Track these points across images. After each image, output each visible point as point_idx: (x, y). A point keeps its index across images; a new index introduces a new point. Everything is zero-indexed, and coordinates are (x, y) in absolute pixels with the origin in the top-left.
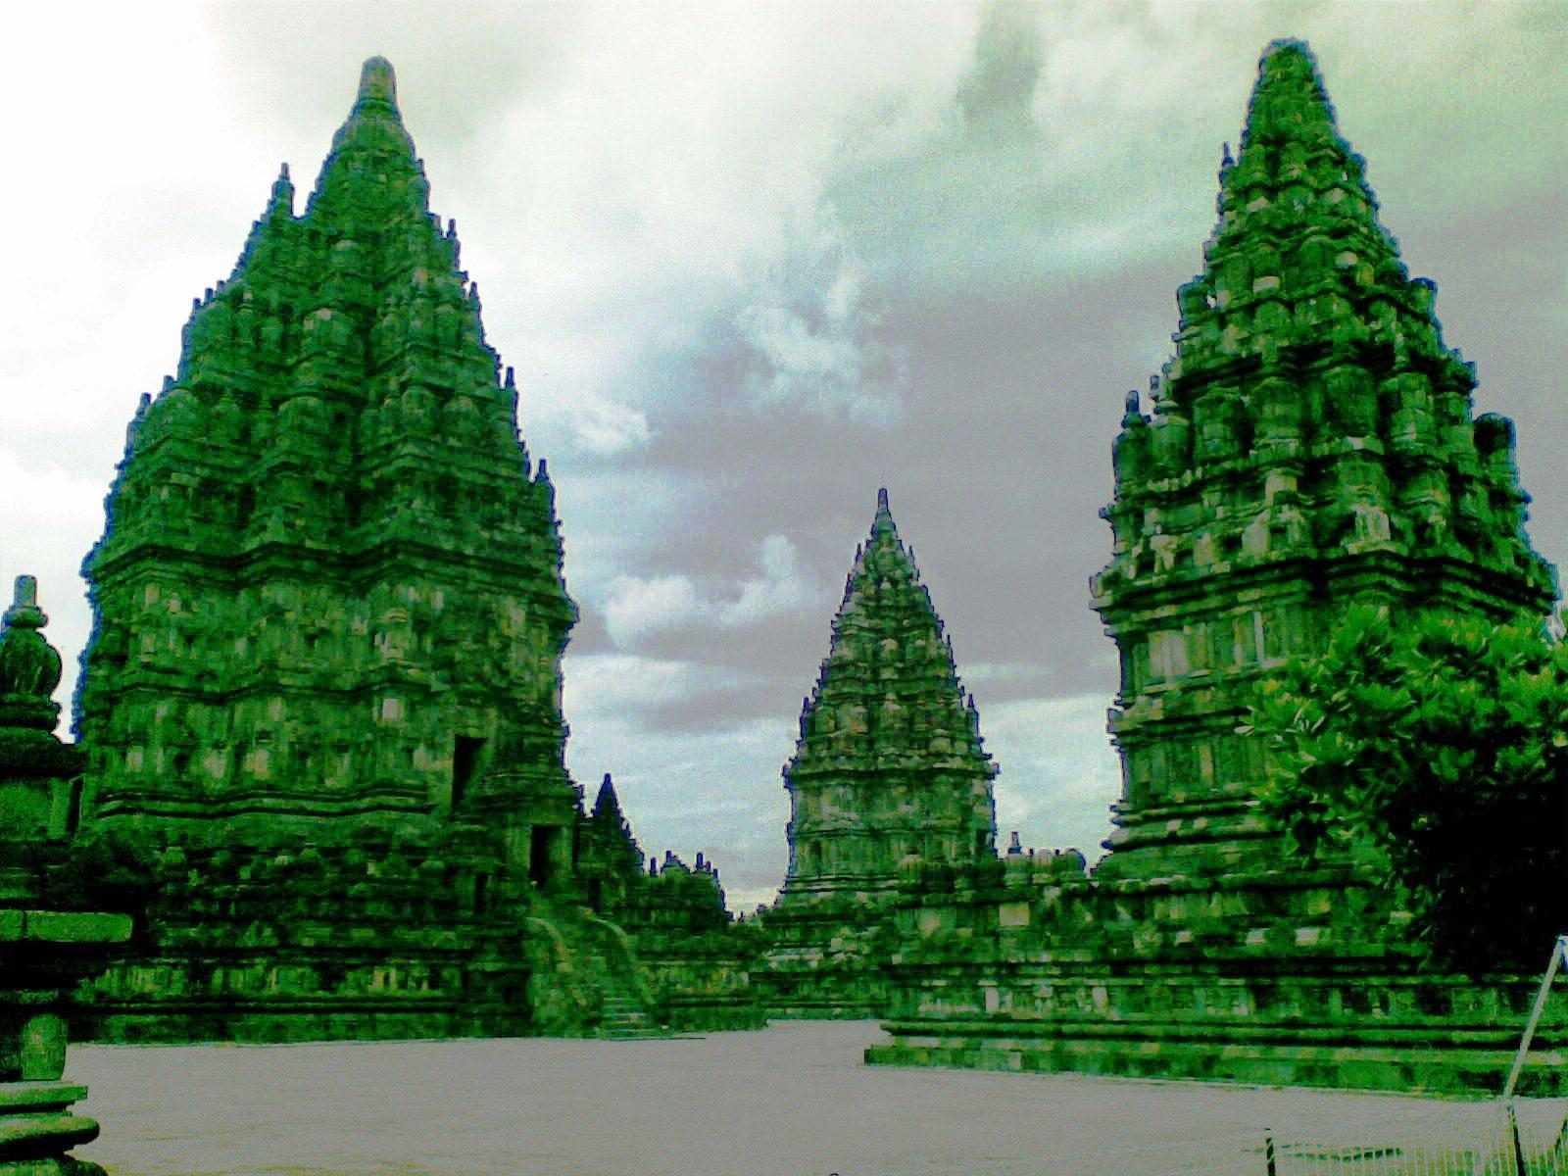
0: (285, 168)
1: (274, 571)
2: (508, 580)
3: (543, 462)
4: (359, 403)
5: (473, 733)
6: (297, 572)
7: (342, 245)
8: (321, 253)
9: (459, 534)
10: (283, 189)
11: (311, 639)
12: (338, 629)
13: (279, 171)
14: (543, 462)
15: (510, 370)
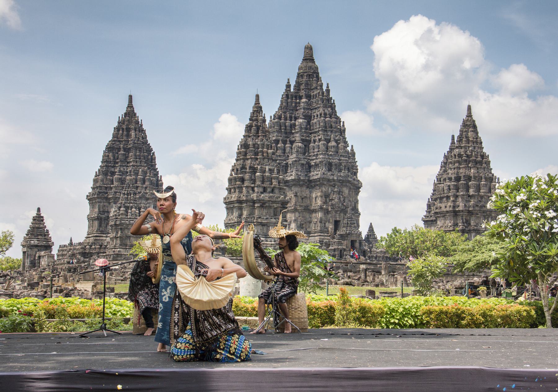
0: (289, 80)
1: (294, 185)
2: (344, 184)
3: (352, 146)
4: (309, 142)
5: (338, 219)
6: (299, 185)
7: (304, 100)
8: (298, 101)
9: (333, 175)
10: (288, 86)
11: (302, 199)
12: (308, 196)
13: (287, 81)
14: (352, 146)
15: (343, 122)
